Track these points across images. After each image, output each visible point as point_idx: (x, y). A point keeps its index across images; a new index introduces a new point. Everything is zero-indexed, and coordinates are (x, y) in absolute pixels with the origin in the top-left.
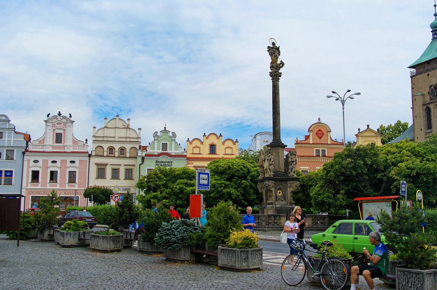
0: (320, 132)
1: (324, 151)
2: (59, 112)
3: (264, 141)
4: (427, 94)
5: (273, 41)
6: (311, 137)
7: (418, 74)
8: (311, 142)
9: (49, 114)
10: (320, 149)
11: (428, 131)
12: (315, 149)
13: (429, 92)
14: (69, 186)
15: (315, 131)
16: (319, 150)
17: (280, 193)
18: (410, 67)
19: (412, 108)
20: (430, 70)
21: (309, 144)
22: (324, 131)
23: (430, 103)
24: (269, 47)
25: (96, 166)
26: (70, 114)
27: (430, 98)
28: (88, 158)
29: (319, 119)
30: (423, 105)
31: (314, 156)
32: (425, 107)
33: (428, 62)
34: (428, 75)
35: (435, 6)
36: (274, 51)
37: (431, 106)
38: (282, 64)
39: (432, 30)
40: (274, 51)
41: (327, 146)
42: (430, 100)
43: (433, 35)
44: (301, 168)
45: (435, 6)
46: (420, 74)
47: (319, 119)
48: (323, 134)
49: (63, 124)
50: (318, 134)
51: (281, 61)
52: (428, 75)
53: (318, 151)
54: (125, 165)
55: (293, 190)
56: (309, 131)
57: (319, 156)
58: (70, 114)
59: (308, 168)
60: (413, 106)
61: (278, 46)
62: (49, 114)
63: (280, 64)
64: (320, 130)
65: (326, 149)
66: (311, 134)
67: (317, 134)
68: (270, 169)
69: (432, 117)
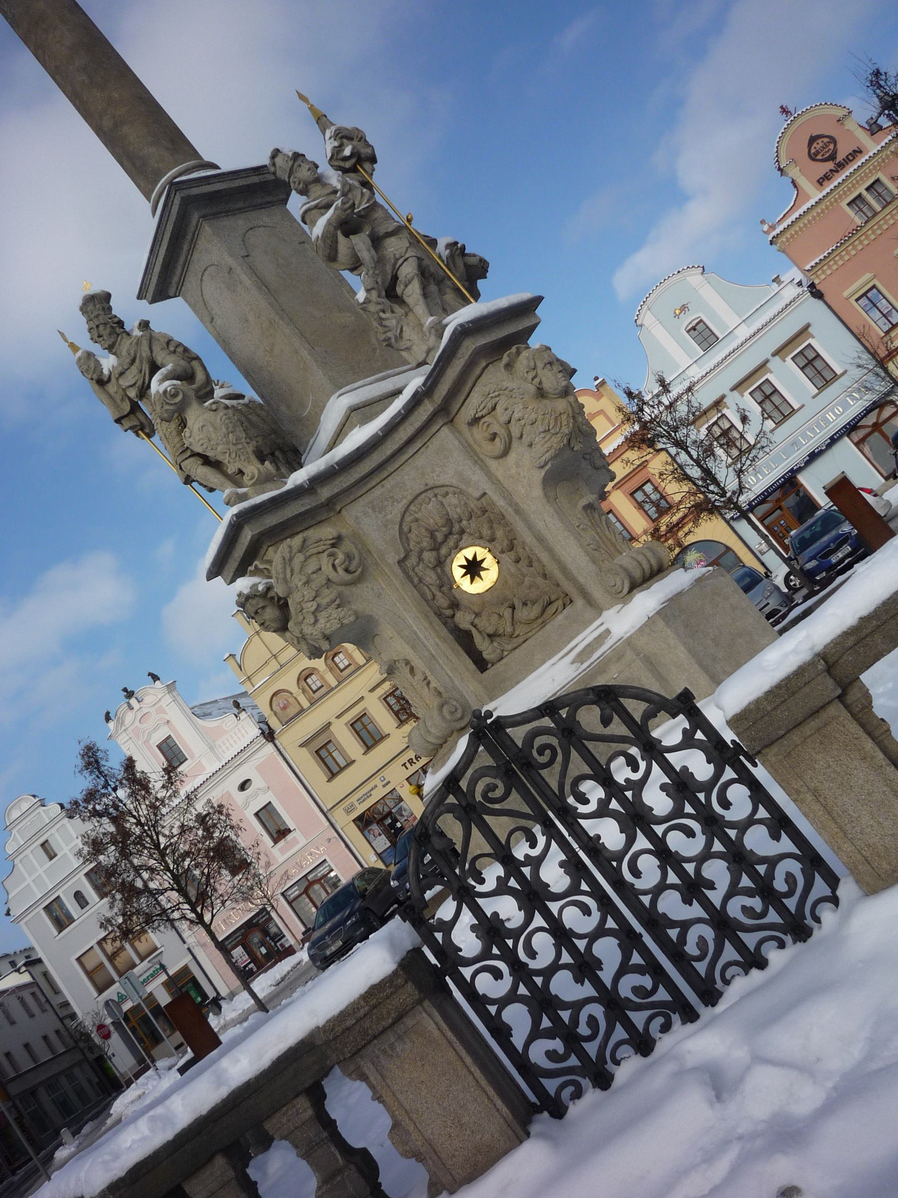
0: (817, 145)
2: (125, 690)
9: (108, 713)
10: (862, 190)
14: (283, 851)
17: (473, 568)
25: (304, 748)
26: (150, 674)
28: (270, 747)
44: (846, 294)
48: (833, 140)
49: (152, 710)
54: (372, 690)
58: (150, 674)
59: (868, 276)
62: (108, 713)
64: (813, 140)
67: (813, 157)
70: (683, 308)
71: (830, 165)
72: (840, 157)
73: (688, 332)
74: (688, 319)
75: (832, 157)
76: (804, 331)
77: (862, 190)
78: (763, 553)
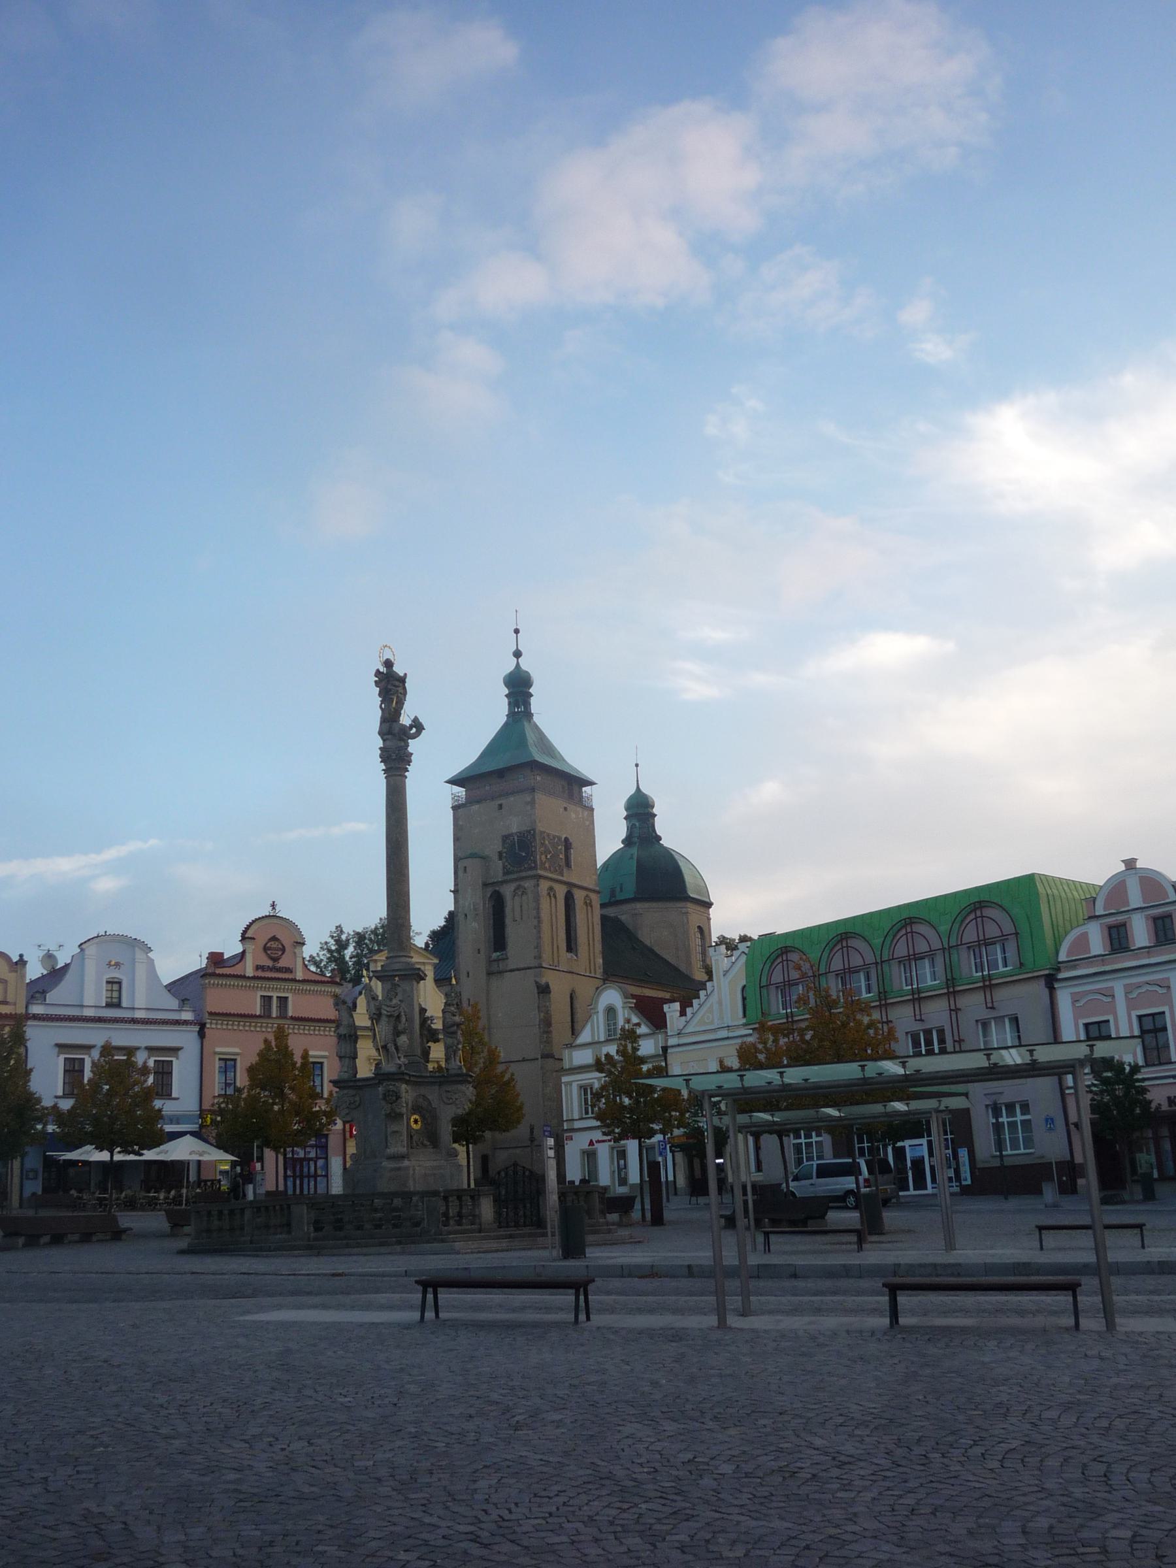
0: (273, 945)
1: (283, 1001)
3: (109, 964)
4: (496, 857)
5: (388, 655)
6: (249, 958)
7: (470, 801)
8: (250, 972)
10: (275, 995)
11: (495, 955)
12: (260, 993)
13: (500, 853)
15: (262, 940)
16: (270, 998)
17: (416, 1121)
18: (452, 782)
19: (455, 892)
20: (507, 794)
21: (244, 977)
22: (287, 943)
23: (502, 882)
24: (378, 673)
27: (504, 867)
29: (273, 905)
30: (485, 885)
31: (256, 1016)
32: (490, 890)
33: (501, 773)
34: (500, 806)
35: (517, 631)
36: (391, 685)
37: (507, 891)
38: (418, 726)
39: (507, 691)
40: (391, 685)
41: (294, 986)
42: (505, 874)
43: (509, 704)
44: (218, 1050)
45: (517, 631)
46: (478, 802)
47: (273, 905)
48: (283, 950)
50: (270, 949)
51: (416, 720)
52: (500, 806)
53: (267, 1000)
55: (460, 1112)
56: (244, 938)
57: (269, 1017)
60: (456, 885)
61: (402, 674)
63: (411, 727)
64: (274, 939)
65: (289, 995)
66: (250, 947)
67: (265, 949)
68: (397, 1048)
69: (508, 920)
70: (117, 965)
71: (270, 963)
72: (282, 963)
73: (108, 982)
74: (115, 974)
75: (275, 960)
76: (175, 1050)
77: (275, 995)
78: (28, 1178)
